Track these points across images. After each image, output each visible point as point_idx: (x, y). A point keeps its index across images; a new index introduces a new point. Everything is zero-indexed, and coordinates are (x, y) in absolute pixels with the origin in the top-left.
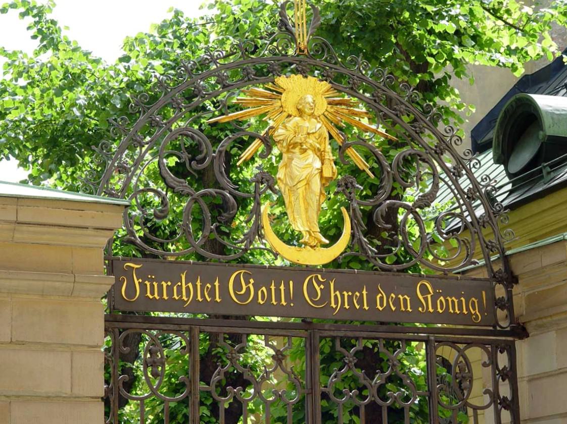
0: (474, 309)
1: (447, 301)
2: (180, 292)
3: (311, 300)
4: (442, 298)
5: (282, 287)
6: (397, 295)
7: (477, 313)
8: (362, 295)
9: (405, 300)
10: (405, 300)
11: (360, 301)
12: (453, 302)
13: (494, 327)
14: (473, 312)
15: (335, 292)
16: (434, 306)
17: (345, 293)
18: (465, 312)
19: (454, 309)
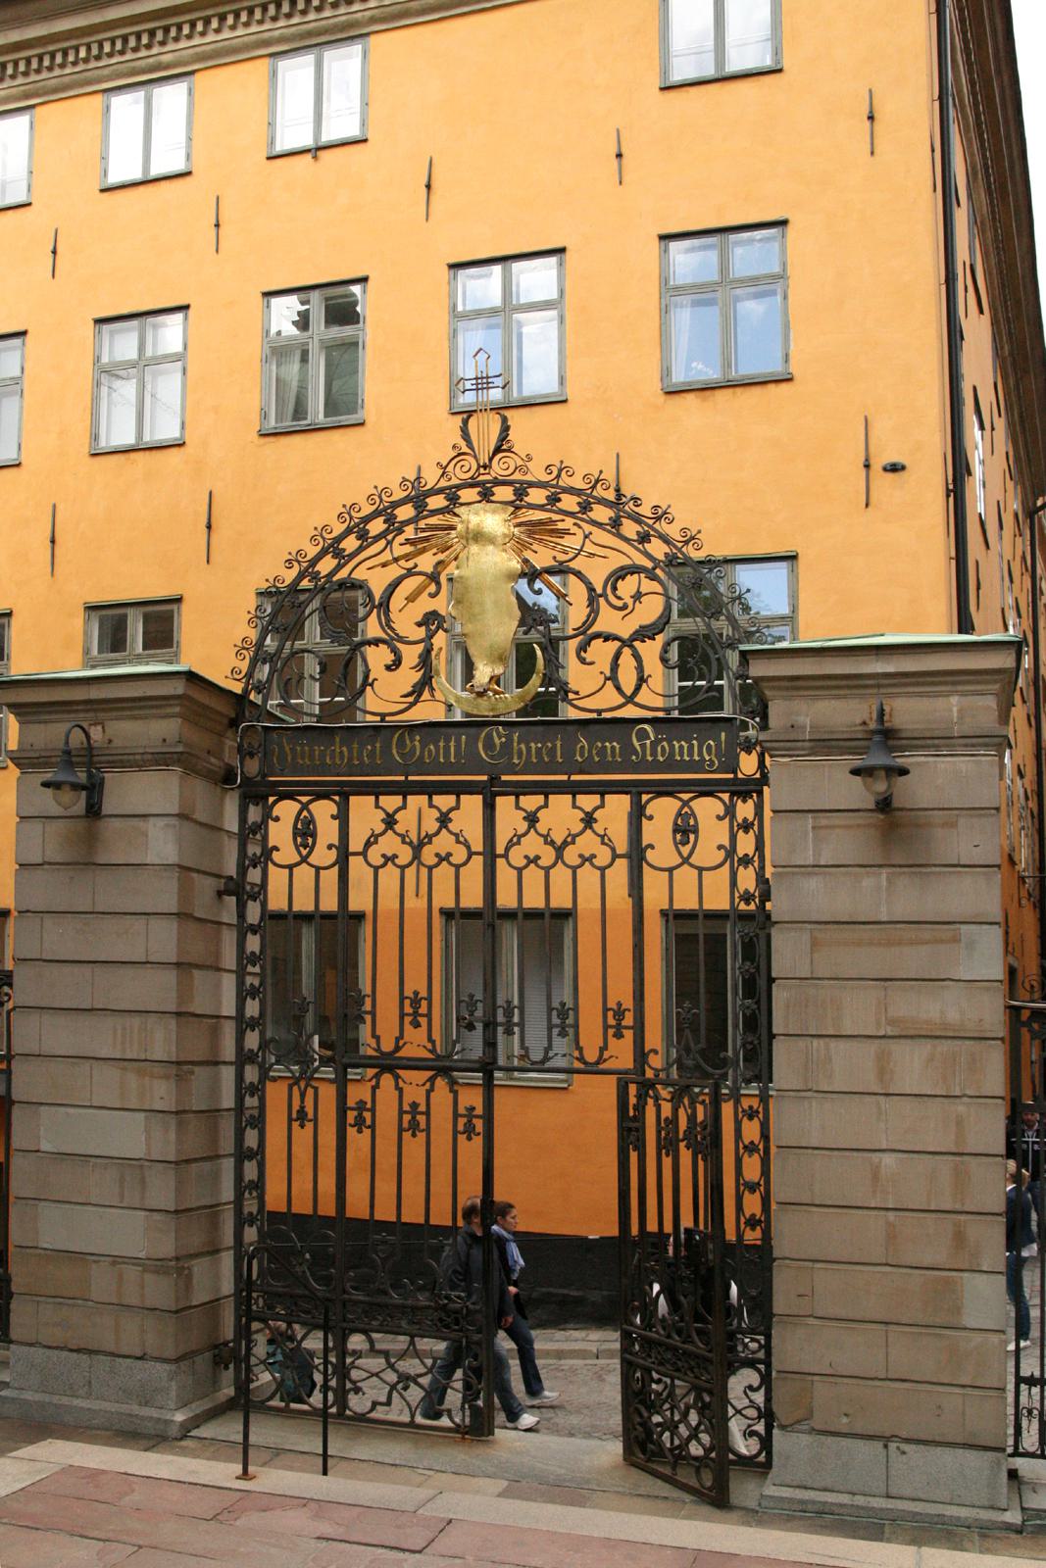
0: (709, 754)
1: (672, 747)
2: (333, 758)
3: (487, 755)
4: (665, 743)
5: (452, 744)
6: (603, 743)
7: (714, 759)
8: (555, 746)
9: (613, 748)
10: (613, 748)
11: (552, 752)
12: (681, 747)
13: (734, 772)
14: (707, 758)
15: (519, 743)
16: (654, 753)
17: (533, 745)
18: (697, 758)
19: (682, 754)
